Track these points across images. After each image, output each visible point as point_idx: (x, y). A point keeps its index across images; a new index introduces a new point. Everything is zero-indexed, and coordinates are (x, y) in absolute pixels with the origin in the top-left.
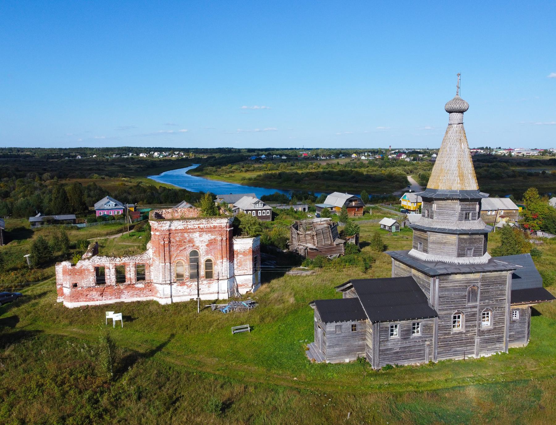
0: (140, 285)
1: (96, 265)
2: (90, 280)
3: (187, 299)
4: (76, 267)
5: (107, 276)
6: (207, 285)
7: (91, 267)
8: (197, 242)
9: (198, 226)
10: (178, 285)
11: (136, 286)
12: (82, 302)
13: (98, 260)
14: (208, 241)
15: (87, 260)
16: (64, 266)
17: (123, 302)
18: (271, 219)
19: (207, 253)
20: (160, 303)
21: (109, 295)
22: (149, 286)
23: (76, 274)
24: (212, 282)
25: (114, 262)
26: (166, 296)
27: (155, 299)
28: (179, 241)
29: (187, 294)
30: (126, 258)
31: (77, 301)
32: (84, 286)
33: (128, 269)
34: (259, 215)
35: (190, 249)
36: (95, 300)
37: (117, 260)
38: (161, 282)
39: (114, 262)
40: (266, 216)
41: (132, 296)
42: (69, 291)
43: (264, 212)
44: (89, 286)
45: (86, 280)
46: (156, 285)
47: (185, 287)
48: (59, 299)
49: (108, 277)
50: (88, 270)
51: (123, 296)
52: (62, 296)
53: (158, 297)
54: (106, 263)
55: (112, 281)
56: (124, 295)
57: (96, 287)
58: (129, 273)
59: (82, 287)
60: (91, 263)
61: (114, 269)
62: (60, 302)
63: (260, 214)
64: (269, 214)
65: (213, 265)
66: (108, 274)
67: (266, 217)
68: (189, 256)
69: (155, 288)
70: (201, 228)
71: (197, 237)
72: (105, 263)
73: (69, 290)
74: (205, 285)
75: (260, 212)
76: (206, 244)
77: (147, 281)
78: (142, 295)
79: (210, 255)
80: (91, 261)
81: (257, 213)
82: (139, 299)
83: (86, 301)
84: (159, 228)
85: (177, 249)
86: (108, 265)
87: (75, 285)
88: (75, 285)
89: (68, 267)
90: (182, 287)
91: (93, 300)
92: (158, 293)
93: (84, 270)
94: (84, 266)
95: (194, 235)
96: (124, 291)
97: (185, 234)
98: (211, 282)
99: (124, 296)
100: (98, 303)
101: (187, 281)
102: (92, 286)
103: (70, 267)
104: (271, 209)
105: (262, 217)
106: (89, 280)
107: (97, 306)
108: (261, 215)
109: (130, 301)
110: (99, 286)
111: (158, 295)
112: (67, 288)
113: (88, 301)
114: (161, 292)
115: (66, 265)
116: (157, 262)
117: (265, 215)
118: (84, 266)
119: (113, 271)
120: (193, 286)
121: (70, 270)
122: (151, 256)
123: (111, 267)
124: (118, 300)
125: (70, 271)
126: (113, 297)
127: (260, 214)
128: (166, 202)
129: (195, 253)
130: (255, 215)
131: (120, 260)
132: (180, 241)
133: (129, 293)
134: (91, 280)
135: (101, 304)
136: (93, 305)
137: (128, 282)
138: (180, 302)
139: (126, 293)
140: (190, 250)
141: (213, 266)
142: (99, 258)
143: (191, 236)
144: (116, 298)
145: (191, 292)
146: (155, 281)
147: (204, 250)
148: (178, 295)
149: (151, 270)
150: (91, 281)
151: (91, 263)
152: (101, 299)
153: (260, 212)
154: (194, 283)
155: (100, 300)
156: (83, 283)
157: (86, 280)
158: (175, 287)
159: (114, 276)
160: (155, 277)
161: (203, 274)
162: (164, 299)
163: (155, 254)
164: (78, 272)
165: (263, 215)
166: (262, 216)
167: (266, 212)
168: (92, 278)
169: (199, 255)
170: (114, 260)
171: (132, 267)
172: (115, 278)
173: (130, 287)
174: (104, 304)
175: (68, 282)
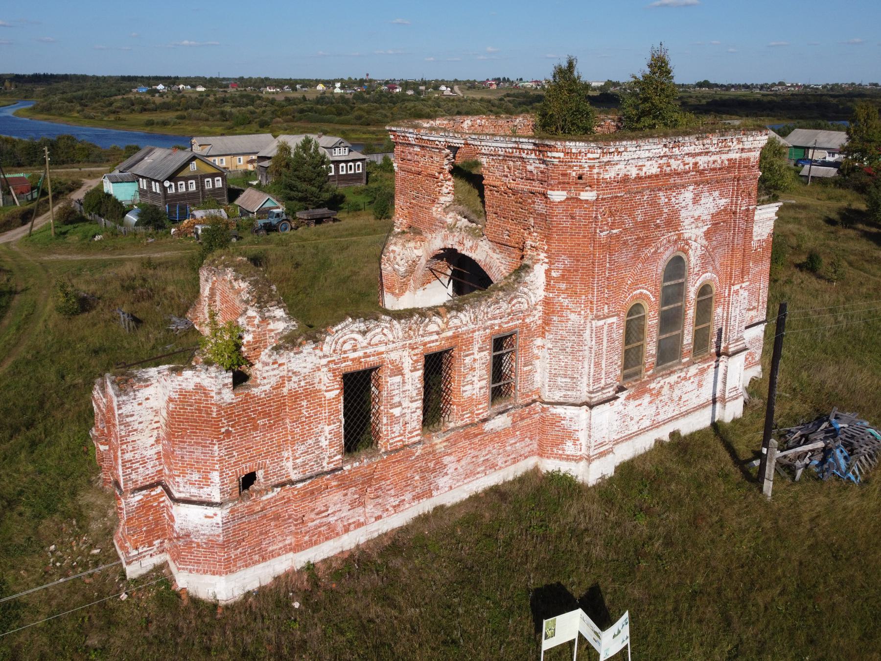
0: (501, 422)
1: (348, 366)
2: (322, 439)
3: (644, 443)
4: (255, 391)
5: (393, 406)
6: (697, 379)
7: (325, 380)
8: (687, 222)
9: (694, 161)
10: (628, 398)
11: (488, 426)
12: (283, 557)
13: (359, 337)
14: (709, 217)
15: (308, 348)
16: (184, 394)
17: (439, 510)
18: (364, 181)
19: (706, 260)
20: (580, 479)
21: (392, 492)
22: (522, 419)
23: (255, 428)
24: (708, 367)
25: (419, 339)
26: (602, 449)
27: (549, 465)
28: (644, 222)
29: (646, 423)
30: (461, 315)
31: (256, 557)
32: (294, 477)
33: (468, 360)
34: (341, 173)
35: (668, 253)
36: (340, 527)
37: (432, 327)
38: (585, 397)
39: (419, 339)
40: (355, 174)
41: (470, 474)
42: (218, 519)
43: (351, 166)
44: (317, 469)
45: (303, 448)
46: (559, 410)
47: (647, 398)
48: (140, 557)
49: (397, 412)
50: (311, 393)
51: (442, 481)
52: (151, 544)
53: (568, 458)
54: (391, 346)
55: (409, 428)
56: (446, 474)
57: (347, 467)
58: (469, 377)
59: (282, 485)
60: (324, 361)
61: (420, 373)
62: (144, 571)
63: (342, 171)
64: (361, 171)
65: (713, 304)
66: (396, 399)
67: (356, 178)
68: (662, 279)
69: (556, 421)
70: (701, 168)
71: (686, 207)
72: (382, 348)
73: (220, 514)
74: (692, 379)
75: (342, 167)
76: (705, 228)
77: (520, 401)
78: (500, 461)
79: (711, 268)
80: (326, 348)
81: (337, 169)
82: (493, 479)
83: (297, 548)
84: (596, 171)
85: (636, 257)
86: (394, 356)
87: (249, 480)
88: (249, 480)
89: (216, 398)
90: (638, 402)
91: (331, 533)
92: (569, 443)
93: (295, 396)
94: (295, 379)
95: (681, 197)
96: (446, 460)
97: (661, 194)
98: (705, 366)
99: (446, 478)
100: (349, 541)
101: (653, 378)
102: (332, 466)
103: (228, 396)
104: (365, 159)
105: (348, 178)
106: (317, 441)
107: (351, 555)
108: (344, 173)
109: (466, 496)
110: (356, 464)
111: (569, 448)
112: (210, 504)
113: (311, 544)
114: (582, 437)
115: (199, 388)
116: (573, 317)
117: (353, 172)
118: (295, 379)
119: (414, 379)
120: (666, 390)
121: (229, 411)
122: (541, 294)
123: (407, 364)
124: (426, 506)
125: (229, 417)
126: (408, 496)
127: (342, 171)
128: (30, 165)
129: (677, 267)
130: (361, 171)
131: (443, 326)
132: (645, 225)
133: (463, 462)
134: (324, 443)
135: (362, 540)
136: (332, 554)
137: (454, 421)
138: (632, 461)
139: (450, 469)
140: (667, 255)
141: (713, 309)
142: (362, 327)
143: (673, 199)
144: (418, 497)
145: (658, 414)
146: (547, 396)
147: (699, 252)
148: (628, 432)
149: (536, 351)
150: (324, 443)
151: (324, 361)
152: (362, 520)
153: (342, 167)
154: (668, 380)
155: (359, 525)
156: (284, 463)
157: (303, 448)
158: (621, 408)
159: (419, 404)
160: (560, 380)
161: (690, 341)
162: (596, 464)
163: (563, 286)
164: (267, 415)
165: (349, 172)
166: (347, 175)
167: (355, 165)
168: (327, 429)
169: (686, 273)
170: (421, 332)
171: (481, 350)
172: (420, 412)
173: (467, 436)
174: (376, 535)
175: (215, 476)
